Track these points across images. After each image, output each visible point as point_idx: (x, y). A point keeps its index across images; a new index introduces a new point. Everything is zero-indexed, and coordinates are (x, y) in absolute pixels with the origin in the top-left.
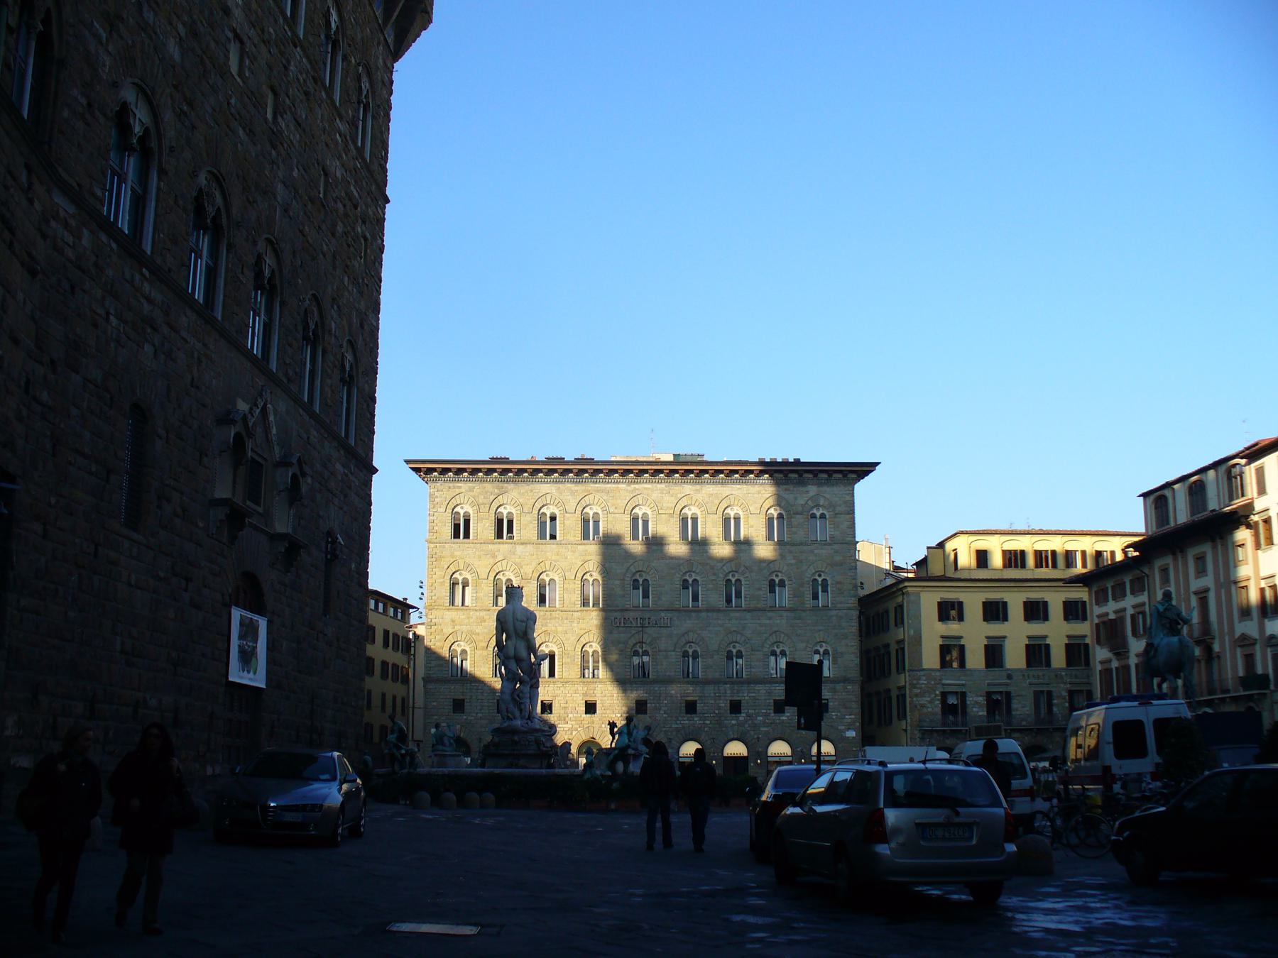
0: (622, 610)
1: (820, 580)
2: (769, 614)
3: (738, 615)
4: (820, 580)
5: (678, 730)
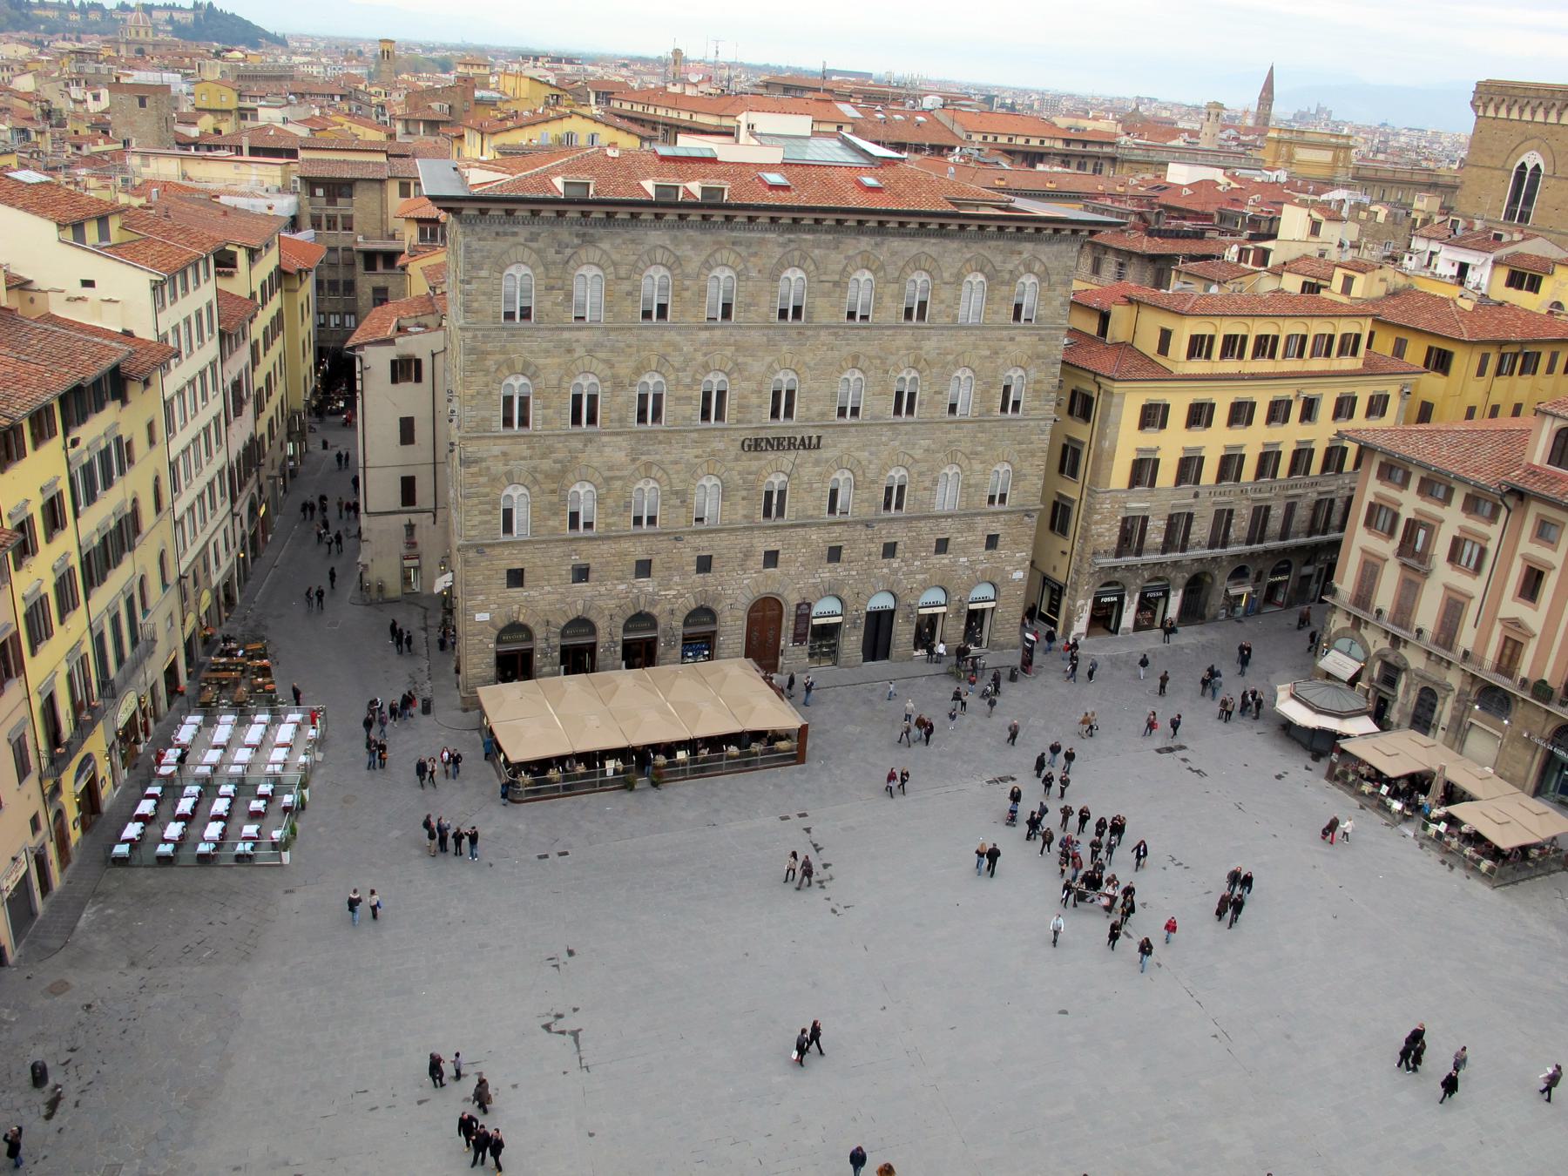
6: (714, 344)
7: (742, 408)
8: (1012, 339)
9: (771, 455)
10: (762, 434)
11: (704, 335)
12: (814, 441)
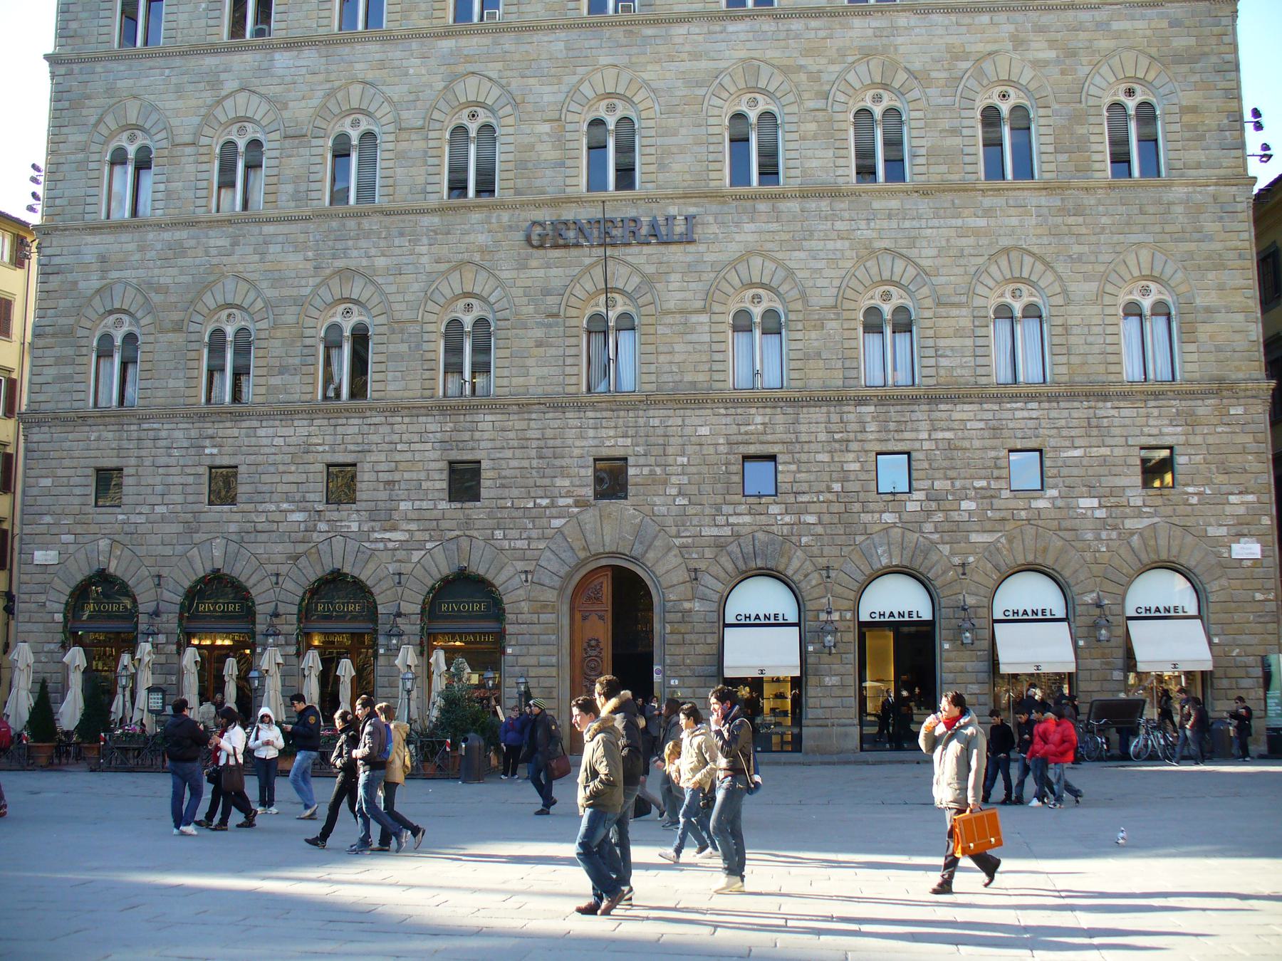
0: (555, 203)
1: (1131, 104)
2: (987, 202)
3: (894, 204)
4: (1131, 104)
5: (719, 545)
6: (468, 59)
7: (522, 165)
8: (1100, 26)
9: (588, 256)
10: (569, 214)
11: (447, 44)
12: (680, 228)
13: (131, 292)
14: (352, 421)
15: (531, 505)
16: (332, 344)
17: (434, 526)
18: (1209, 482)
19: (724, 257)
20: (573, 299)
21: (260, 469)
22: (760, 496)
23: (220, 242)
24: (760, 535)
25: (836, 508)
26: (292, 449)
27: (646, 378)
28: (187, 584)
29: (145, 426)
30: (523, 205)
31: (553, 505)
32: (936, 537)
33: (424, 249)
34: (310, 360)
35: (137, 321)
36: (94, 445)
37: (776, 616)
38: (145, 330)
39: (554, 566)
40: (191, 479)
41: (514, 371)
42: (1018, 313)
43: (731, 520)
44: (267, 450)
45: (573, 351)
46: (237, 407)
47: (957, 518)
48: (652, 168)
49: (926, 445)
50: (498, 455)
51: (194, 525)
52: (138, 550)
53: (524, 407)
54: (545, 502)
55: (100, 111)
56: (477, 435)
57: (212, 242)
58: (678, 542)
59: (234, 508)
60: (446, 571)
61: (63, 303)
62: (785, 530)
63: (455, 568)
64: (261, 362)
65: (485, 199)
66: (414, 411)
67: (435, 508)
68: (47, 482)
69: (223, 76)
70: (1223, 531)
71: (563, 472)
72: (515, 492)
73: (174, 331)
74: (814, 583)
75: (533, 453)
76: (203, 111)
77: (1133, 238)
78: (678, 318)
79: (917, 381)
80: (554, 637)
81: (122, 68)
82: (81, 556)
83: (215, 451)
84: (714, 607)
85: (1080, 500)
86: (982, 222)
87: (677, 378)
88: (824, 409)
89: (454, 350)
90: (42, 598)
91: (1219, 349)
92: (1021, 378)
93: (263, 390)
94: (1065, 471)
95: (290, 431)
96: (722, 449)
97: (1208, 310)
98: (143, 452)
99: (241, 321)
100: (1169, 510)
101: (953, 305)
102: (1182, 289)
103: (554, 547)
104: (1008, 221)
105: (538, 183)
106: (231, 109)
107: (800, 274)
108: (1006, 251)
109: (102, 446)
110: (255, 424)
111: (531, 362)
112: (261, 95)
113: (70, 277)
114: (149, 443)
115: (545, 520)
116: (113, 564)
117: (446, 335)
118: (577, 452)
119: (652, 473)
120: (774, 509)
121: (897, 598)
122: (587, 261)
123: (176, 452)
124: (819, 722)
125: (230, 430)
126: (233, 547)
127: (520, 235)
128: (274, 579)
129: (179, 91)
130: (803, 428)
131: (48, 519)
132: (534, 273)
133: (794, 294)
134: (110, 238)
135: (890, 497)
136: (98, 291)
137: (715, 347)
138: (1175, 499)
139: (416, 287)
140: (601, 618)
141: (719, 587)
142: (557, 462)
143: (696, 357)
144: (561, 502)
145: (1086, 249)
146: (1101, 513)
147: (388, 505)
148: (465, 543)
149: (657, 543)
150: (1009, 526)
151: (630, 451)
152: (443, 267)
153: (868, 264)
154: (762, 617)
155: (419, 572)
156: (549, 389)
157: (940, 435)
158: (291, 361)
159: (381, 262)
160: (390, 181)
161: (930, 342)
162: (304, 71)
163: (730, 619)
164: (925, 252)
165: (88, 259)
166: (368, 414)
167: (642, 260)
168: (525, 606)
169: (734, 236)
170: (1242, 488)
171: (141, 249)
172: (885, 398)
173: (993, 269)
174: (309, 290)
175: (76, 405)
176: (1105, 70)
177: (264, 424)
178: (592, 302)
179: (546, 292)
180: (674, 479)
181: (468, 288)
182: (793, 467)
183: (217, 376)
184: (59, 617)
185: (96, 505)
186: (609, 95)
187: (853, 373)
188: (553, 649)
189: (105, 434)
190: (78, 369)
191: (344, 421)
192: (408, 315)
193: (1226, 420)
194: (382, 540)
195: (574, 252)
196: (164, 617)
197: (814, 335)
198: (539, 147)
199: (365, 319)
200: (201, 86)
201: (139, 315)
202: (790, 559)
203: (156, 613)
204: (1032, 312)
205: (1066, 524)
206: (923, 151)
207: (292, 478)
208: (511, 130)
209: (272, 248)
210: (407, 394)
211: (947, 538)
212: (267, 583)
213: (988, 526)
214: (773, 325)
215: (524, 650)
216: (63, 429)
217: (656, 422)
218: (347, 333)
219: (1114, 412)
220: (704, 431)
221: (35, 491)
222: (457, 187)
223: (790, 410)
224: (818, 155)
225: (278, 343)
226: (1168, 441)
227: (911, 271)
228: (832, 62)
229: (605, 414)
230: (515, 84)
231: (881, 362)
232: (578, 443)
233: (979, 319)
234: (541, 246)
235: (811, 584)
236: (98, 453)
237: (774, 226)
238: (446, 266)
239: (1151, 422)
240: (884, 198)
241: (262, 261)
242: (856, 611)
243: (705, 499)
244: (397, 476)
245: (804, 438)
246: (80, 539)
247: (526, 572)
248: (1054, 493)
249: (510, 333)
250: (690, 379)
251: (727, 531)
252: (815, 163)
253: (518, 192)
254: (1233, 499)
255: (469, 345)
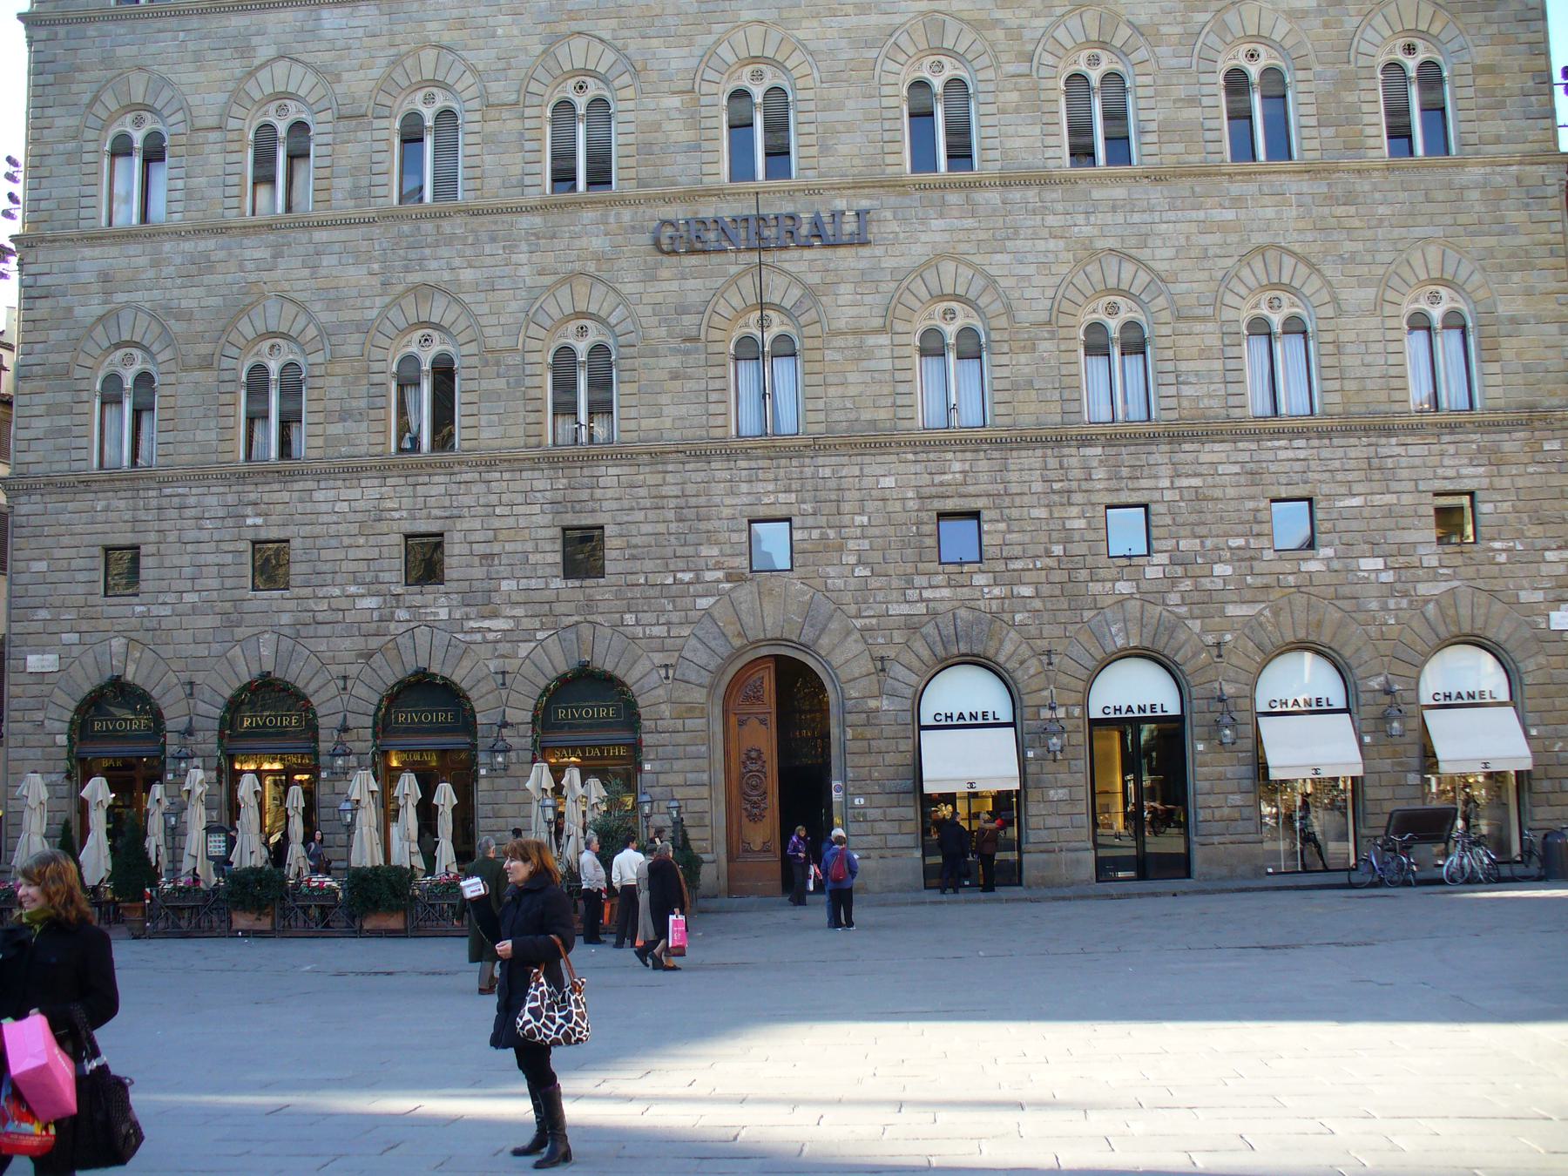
0: (691, 196)
1: (1411, 64)
2: (1236, 189)
3: (1119, 192)
4: (1411, 64)
5: (912, 626)
7: (645, 149)
9: (733, 263)
10: (707, 210)
12: (850, 226)
13: (143, 320)
14: (436, 479)
15: (670, 580)
16: (407, 382)
17: (546, 610)
18: (1520, 535)
19: (902, 262)
20: (716, 318)
21: (320, 543)
22: (961, 564)
23: (258, 254)
24: (962, 613)
25: (1057, 576)
26: (359, 517)
27: (812, 417)
28: (228, 693)
29: (168, 491)
30: (649, 199)
31: (698, 580)
32: (1183, 610)
33: (523, 258)
34: (380, 402)
35: (153, 356)
36: (101, 517)
37: (984, 714)
38: (163, 368)
39: (702, 657)
40: (229, 558)
41: (643, 411)
42: (1277, 327)
43: (927, 594)
44: (325, 518)
45: (718, 384)
46: (286, 465)
47: (1209, 586)
48: (814, 151)
49: (1168, 496)
50: (626, 519)
51: (234, 617)
52: (159, 649)
53: (657, 457)
54: (687, 577)
55: (95, 87)
56: (598, 493)
57: (248, 254)
58: (859, 623)
59: (287, 594)
60: (563, 668)
61: (54, 336)
62: (995, 605)
63: (574, 664)
64: (315, 406)
65: (599, 193)
66: (516, 465)
67: (547, 588)
68: (42, 566)
69: (255, 41)
70: (1539, 596)
71: (710, 538)
72: (649, 565)
73: (201, 368)
74: (1032, 671)
75: (671, 515)
76: (231, 86)
77: (1419, 232)
78: (851, 340)
79: (1153, 415)
80: (704, 749)
81: (122, 31)
82: (89, 659)
83: (259, 521)
84: (907, 704)
85: (1361, 561)
86: (1230, 215)
87: (852, 416)
88: (1039, 452)
89: (564, 384)
90: (39, 716)
91: (1527, 369)
92: (1283, 409)
93: (319, 442)
94: (1341, 525)
95: (356, 493)
96: (911, 504)
97: (1514, 320)
98: (166, 525)
99: (288, 353)
100: (1471, 572)
101: (1196, 318)
102: (1481, 294)
103: (700, 633)
104: (1261, 212)
105: (667, 171)
106: (267, 82)
107: (1003, 283)
108: (1261, 250)
109: (113, 519)
110: (311, 485)
111: (664, 399)
112: (305, 64)
113: (63, 302)
114: (174, 513)
115: (689, 600)
116: (131, 669)
117: (555, 367)
118: (726, 512)
119: (824, 537)
120: (979, 580)
121: (1137, 689)
122: (733, 270)
123: (208, 524)
124: (1043, 847)
125: (276, 494)
126: (286, 644)
127: (646, 239)
128: (341, 683)
129: (198, 59)
130: (1014, 476)
131: (43, 614)
132: (666, 286)
133: (997, 307)
134: (114, 251)
135: (1125, 562)
136: (101, 318)
137: (899, 376)
138: (1479, 557)
139: (514, 306)
140: (763, 722)
141: (913, 679)
142: (703, 526)
143: (876, 389)
144: (709, 576)
145: (1359, 246)
146: (1388, 577)
147: (486, 585)
148: (586, 630)
149: (833, 625)
150: (1275, 595)
151: (795, 510)
152: (548, 280)
153: (1089, 269)
154: (967, 716)
155: (528, 669)
156: (689, 433)
157: (1185, 482)
158: (355, 403)
159: (467, 275)
160: (477, 172)
161: (1169, 366)
162: (360, 32)
163: (927, 719)
164: (1159, 253)
165: (86, 277)
166: (456, 469)
167: (803, 266)
168: (666, 710)
169: (919, 235)
170: (1561, 542)
171: (156, 264)
172: (1115, 437)
173: (1245, 272)
174: (375, 312)
175: (76, 465)
176: (1378, 21)
177: (322, 485)
178: (741, 322)
179: (682, 310)
180: (852, 545)
181: (581, 307)
182: (1002, 526)
183: (258, 425)
184: (62, 739)
185: (106, 595)
186: (755, 59)
187: (1074, 407)
188: (704, 763)
189: (116, 503)
190: (77, 420)
191: (426, 479)
192: (504, 342)
193: (1539, 457)
194: (479, 630)
195: (716, 259)
196: (200, 736)
197: (1023, 358)
198: (667, 126)
199: (450, 348)
200: (227, 53)
201: (155, 349)
202: (1001, 642)
203: (190, 731)
204: (1294, 326)
205: (1346, 591)
206: (1153, 126)
207: (360, 554)
208: (630, 105)
209: (326, 261)
210: (508, 443)
211: (1197, 612)
212: (332, 689)
213: (1248, 595)
214: (971, 348)
215: (667, 766)
216: (61, 497)
217: (827, 472)
218: (426, 367)
219: (1401, 450)
220: (888, 482)
221: (24, 578)
222: (563, 177)
223: (996, 454)
224: (1019, 131)
225: (337, 381)
226: (1468, 485)
227: (1143, 277)
228: (1036, 15)
229: (761, 463)
230: (633, 47)
231: (1107, 391)
232: (728, 501)
233: (1229, 336)
234: (674, 252)
235: (1028, 673)
236: (107, 527)
237: (969, 223)
238: (554, 278)
239: (1447, 462)
240: (1106, 185)
241: (313, 277)
242: (1085, 706)
243: (890, 569)
244: (496, 548)
245: (1014, 489)
246: (87, 638)
247: (666, 666)
248: (1329, 552)
249: (637, 362)
250: (869, 417)
251: (921, 608)
252: (1018, 143)
253: (642, 183)
254: (1549, 555)
255: (585, 380)
